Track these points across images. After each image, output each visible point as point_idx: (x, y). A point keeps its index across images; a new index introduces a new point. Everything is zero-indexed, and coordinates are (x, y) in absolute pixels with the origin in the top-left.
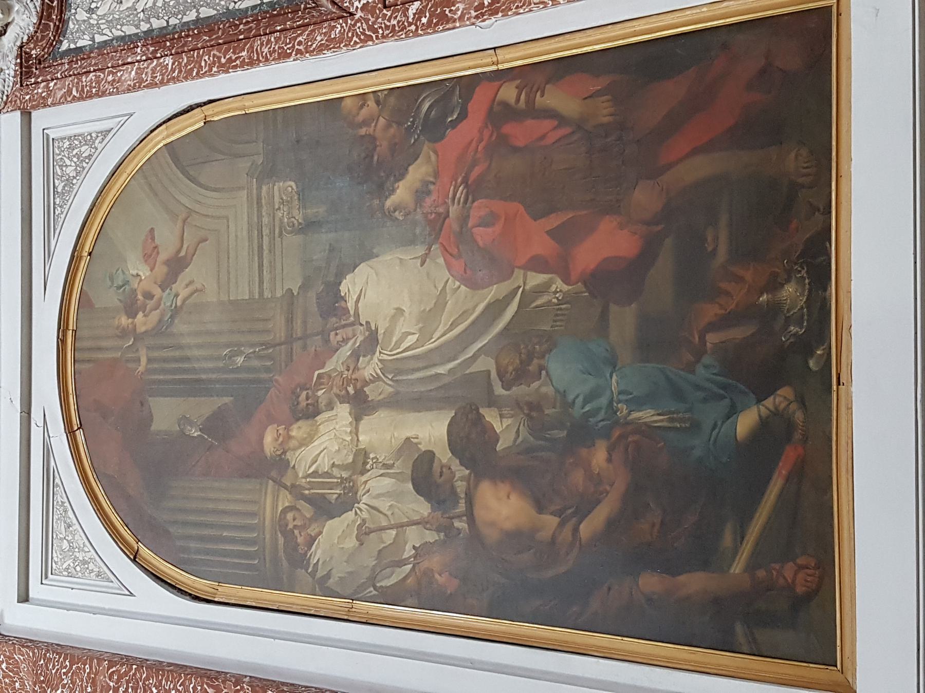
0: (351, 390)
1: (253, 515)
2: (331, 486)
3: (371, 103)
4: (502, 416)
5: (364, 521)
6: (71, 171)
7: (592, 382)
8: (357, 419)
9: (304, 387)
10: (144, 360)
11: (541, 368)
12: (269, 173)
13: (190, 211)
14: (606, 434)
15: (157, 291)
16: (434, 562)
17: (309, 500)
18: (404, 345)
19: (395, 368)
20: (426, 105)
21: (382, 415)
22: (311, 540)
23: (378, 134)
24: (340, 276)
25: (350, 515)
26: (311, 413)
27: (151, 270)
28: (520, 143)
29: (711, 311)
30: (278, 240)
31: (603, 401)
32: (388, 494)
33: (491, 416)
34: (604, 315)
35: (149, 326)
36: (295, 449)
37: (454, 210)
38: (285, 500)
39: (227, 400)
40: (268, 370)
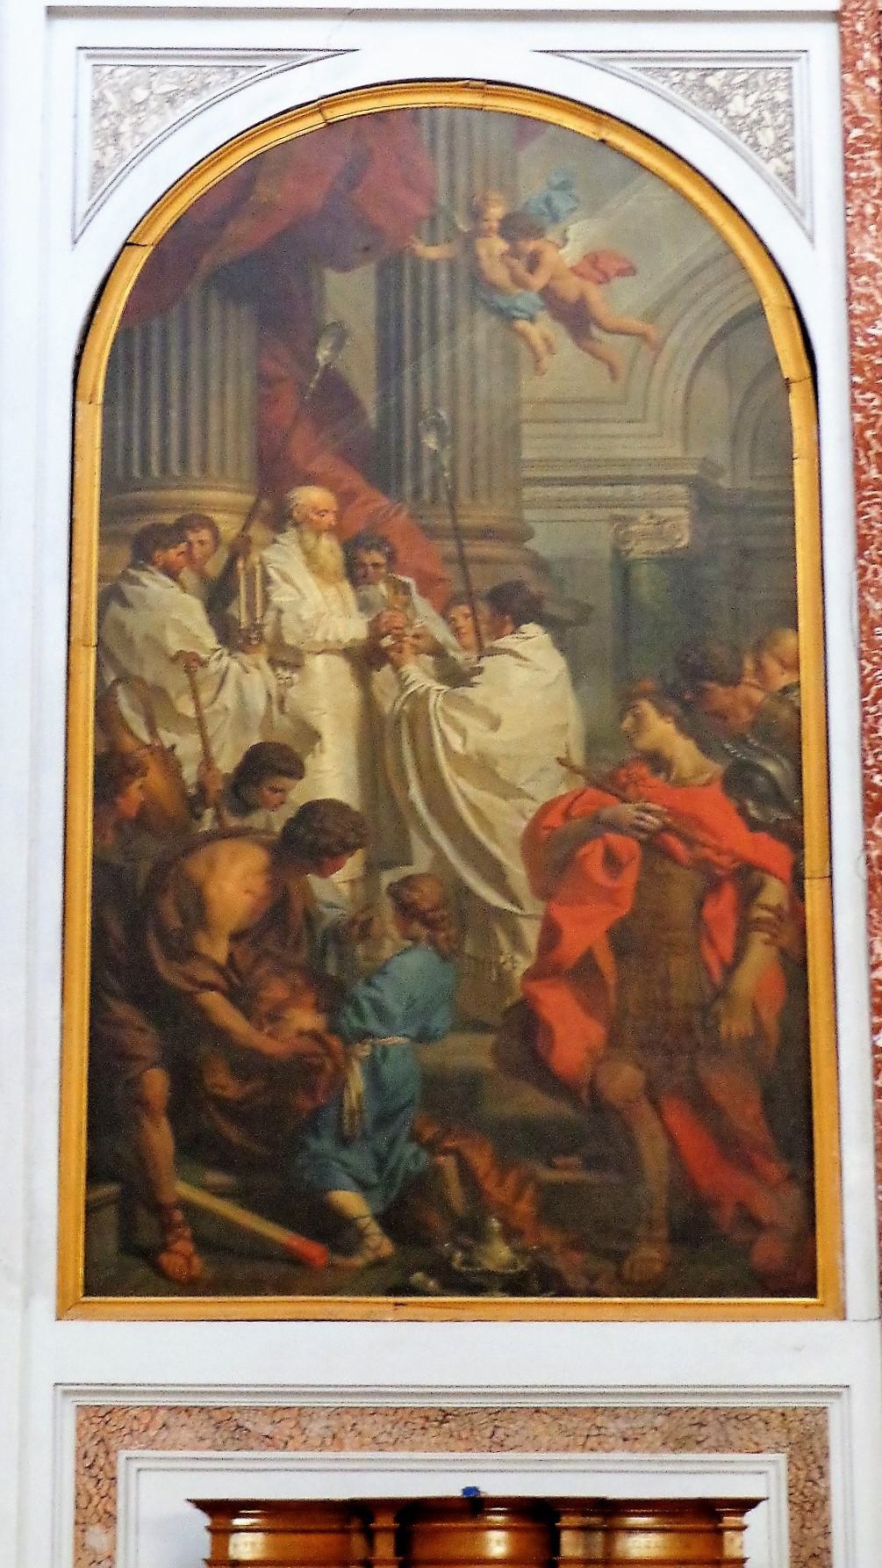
0: (387, 642)
1: (204, 467)
2: (251, 607)
3: (784, 680)
4: (352, 882)
5: (204, 664)
6: (738, 105)
7: (396, 1008)
8: (347, 653)
9: (391, 557)
10: (432, 253)
11: (415, 940)
12: (705, 500)
13: (658, 348)
14: (333, 1029)
15: (539, 280)
16: (155, 778)
17: (230, 568)
18: (448, 729)
19: (417, 716)
20: (772, 768)
21: (351, 694)
22: (172, 573)
23: (742, 690)
24: (548, 623)
25: (210, 639)
26: (355, 573)
27: (573, 270)
28: (710, 911)
29: (481, 1161)
30: (604, 513)
31: (373, 1024)
32: (242, 702)
33: (352, 866)
34: (481, 1027)
35: (485, 264)
36: (301, 542)
37: (628, 811)
38: (229, 526)
39: (372, 415)
40: (417, 492)
